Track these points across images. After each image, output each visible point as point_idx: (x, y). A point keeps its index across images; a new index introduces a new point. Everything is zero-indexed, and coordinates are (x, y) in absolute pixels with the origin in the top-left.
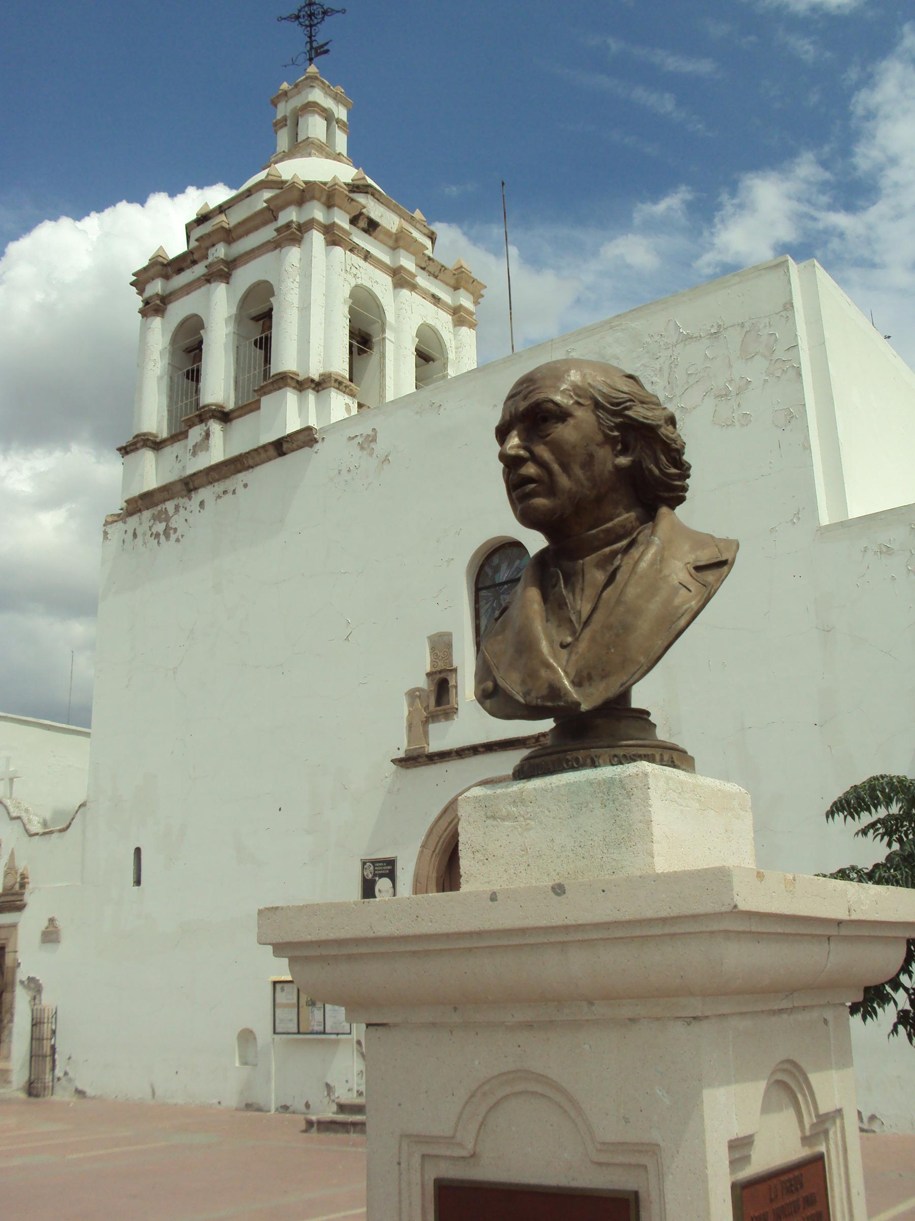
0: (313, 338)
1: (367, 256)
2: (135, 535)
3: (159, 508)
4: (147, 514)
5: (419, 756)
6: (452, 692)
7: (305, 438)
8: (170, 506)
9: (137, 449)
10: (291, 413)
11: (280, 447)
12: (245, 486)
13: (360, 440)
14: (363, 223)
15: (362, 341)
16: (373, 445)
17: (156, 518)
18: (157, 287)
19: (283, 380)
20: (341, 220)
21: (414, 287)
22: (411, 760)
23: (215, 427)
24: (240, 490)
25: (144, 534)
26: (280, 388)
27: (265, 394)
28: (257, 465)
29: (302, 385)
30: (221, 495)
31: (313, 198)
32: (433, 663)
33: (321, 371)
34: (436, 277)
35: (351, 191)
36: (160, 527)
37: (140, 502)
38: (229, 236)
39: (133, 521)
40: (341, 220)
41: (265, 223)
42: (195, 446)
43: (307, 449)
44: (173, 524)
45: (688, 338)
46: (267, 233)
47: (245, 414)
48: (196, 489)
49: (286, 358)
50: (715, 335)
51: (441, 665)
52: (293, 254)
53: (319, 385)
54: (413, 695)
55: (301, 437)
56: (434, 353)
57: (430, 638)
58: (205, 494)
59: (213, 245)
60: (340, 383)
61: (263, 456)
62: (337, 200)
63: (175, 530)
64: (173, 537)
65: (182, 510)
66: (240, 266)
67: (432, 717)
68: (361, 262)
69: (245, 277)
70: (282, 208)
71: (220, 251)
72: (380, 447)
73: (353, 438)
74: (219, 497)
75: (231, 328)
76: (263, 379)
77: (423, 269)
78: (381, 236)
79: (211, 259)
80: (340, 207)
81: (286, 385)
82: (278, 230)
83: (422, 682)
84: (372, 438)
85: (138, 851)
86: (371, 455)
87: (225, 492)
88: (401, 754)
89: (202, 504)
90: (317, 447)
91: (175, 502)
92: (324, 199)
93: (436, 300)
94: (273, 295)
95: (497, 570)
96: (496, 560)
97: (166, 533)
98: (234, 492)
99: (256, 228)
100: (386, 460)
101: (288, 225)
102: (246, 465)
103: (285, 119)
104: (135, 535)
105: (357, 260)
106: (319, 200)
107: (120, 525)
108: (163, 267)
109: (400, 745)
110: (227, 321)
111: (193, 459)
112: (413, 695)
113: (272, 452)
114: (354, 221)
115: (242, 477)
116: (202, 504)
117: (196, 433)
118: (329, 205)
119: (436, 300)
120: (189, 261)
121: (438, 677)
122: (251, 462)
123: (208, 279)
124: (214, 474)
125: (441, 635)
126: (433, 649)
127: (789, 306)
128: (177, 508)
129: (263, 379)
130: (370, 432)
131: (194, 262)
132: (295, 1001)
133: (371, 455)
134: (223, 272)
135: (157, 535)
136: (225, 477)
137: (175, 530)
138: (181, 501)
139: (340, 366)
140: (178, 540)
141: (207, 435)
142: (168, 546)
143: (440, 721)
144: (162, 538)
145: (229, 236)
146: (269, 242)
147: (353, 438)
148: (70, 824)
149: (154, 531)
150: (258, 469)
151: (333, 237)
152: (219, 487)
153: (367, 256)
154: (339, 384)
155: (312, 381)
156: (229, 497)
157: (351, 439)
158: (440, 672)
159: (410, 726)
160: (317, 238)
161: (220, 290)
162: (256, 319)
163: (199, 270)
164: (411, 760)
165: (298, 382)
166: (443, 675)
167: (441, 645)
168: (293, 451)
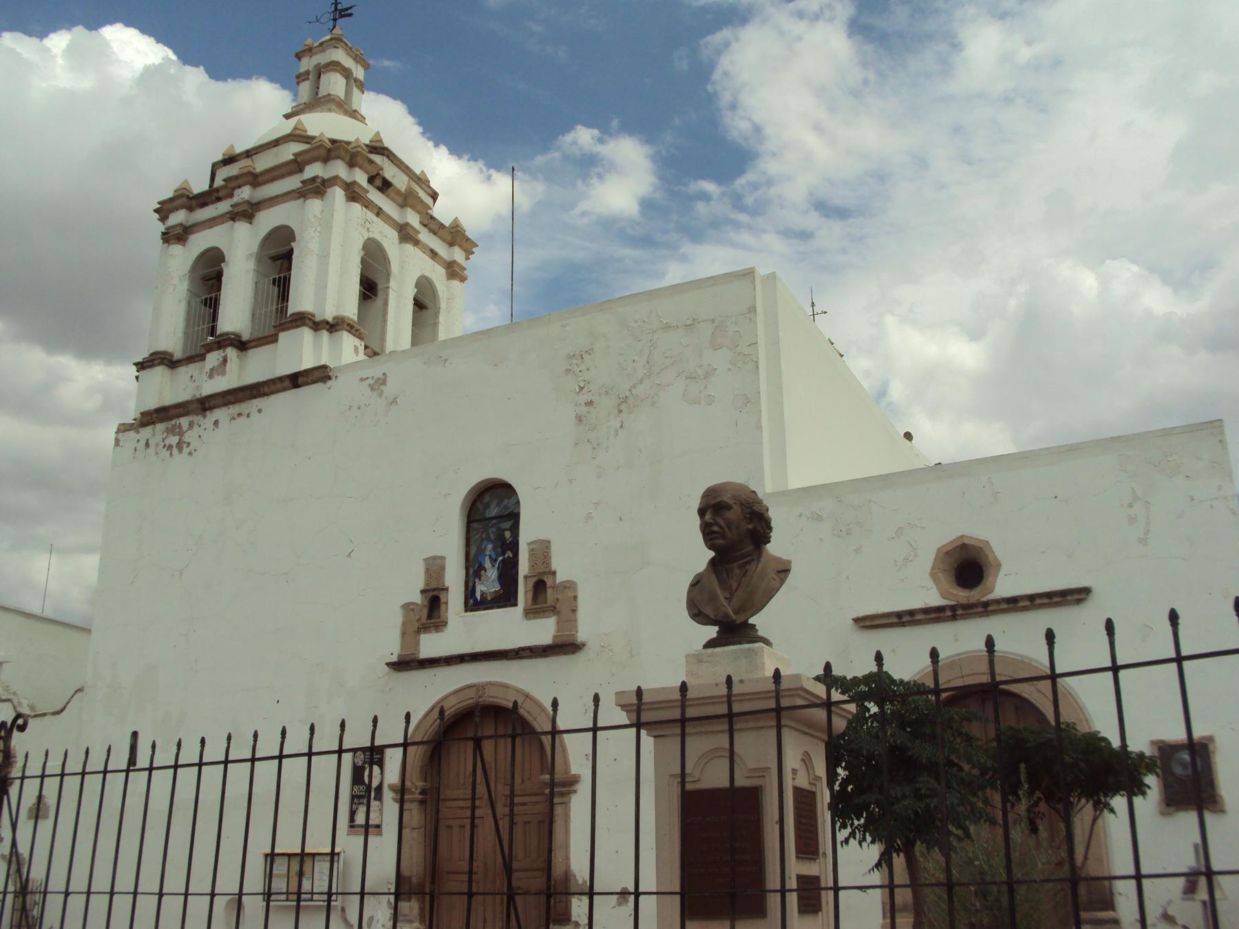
0: (325, 284)
1: (379, 212)
2: (147, 445)
3: (173, 422)
4: (160, 427)
5: (412, 661)
6: (443, 607)
7: (320, 375)
8: (184, 421)
10: (301, 349)
11: (296, 380)
12: (260, 411)
13: (371, 381)
14: (378, 182)
15: (370, 289)
16: (382, 387)
17: (171, 431)
18: (178, 217)
19: (301, 319)
20: (361, 178)
21: (416, 243)
22: (405, 664)
23: (231, 352)
24: (254, 414)
26: (298, 327)
27: (283, 330)
28: (273, 393)
29: (318, 326)
31: (338, 157)
32: (427, 582)
33: (335, 314)
34: (435, 234)
35: (371, 152)
36: (174, 440)
38: (256, 180)
39: (146, 432)
40: (361, 178)
41: (290, 173)
42: (212, 370)
43: (320, 384)
44: (186, 438)
45: (668, 327)
46: (293, 183)
48: (211, 408)
49: (302, 299)
50: (689, 327)
51: (433, 585)
52: (315, 205)
53: (333, 326)
56: (427, 302)
58: (220, 414)
60: (352, 327)
61: (279, 386)
62: (359, 160)
63: (189, 444)
64: (186, 450)
65: (196, 428)
67: (424, 629)
68: (374, 217)
69: (268, 220)
70: (310, 162)
71: (245, 193)
72: (389, 390)
74: (233, 418)
75: (251, 265)
76: (280, 317)
77: (425, 226)
78: (393, 195)
79: (235, 200)
80: (361, 168)
81: (304, 324)
82: (303, 182)
83: (417, 598)
84: (383, 381)
85: (135, 734)
86: (380, 395)
87: (240, 415)
88: (394, 659)
89: (216, 423)
90: (330, 383)
91: (190, 418)
92: (348, 159)
93: (433, 254)
94: (293, 239)
95: (487, 506)
96: (487, 498)
97: (180, 446)
98: (248, 416)
99: (282, 177)
100: (394, 402)
101: (314, 179)
103: (307, 73)
104: (147, 445)
105: (371, 216)
106: (343, 159)
107: (132, 434)
108: (186, 200)
109: (393, 650)
110: (249, 257)
111: (210, 382)
112: (408, 607)
113: (287, 383)
114: (371, 180)
115: (257, 403)
116: (216, 423)
117: (213, 358)
118: (351, 164)
119: (433, 254)
121: (431, 594)
122: (266, 390)
123: (233, 216)
124: (231, 398)
125: (435, 558)
126: (427, 570)
127: (753, 309)
128: (191, 425)
129: (280, 317)
130: (381, 376)
131: (219, 199)
132: (285, 871)
133: (380, 395)
134: (247, 213)
135: (170, 447)
136: (241, 401)
137: (189, 444)
138: (197, 419)
139: (350, 310)
140: (190, 454)
141: (225, 361)
142: (180, 459)
144: (175, 451)
145: (256, 180)
146: (293, 191)
148: (64, 708)
149: (167, 442)
150: (272, 397)
151: (353, 194)
152: (234, 409)
153: (379, 212)
154: (351, 328)
155: (327, 323)
156: (242, 420)
157: (362, 380)
158: (434, 590)
159: (404, 634)
160: (338, 193)
161: (242, 227)
162: (274, 258)
163: (224, 207)
164: (405, 664)
165: (314, 322)
167: (435, 567)
168: (307, 384)
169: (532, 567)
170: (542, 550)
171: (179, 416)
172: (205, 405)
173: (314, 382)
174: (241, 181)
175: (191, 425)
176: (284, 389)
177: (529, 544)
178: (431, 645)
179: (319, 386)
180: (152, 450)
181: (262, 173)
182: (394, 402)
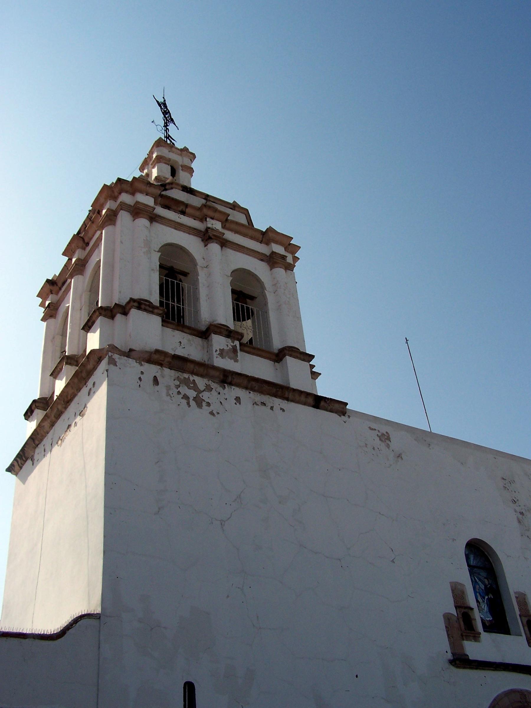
2: (156, 381)
3: (186, 376)
8: (201, 382)
9: (152, 312)
11: (319, 402)
17: (186, 382)
25: (168, 388)
28: (292, 401)
30: (259, 403)
36: (192, 394)
37: (168, 359)
39: (152, 370)
47: (253, 354)
48: (231, 384)
54: (447, 617)
55: (337, 406)
57: (450, 583)
59: (212, 218)
65: (214, 392)
66: (229, 248)
71: (217, 225)
73: (372, 429)
74: (255, 403)
81: (284, 356)
87: (263, 404)
100: (399, 456)
102: (286, 396)
104: (156, 381)
111: (220, 358)
112: (447, 617)
113: (310, 400)
115: (277, 402)
120: (180, 209)
121: (463, 610)
122: (291, 396)
124: (266, 387)
131: (183, 213)
135: (185, 397)
136: (261, 392)
137: (209, 404)
138: (214, 385)
140: (212, 413)
143: (471, 640)
144: (192, 403)
147: (372, 429)
152: (259, 398)
156: (267, 409)
157: (370, 428)
166: (466, 610)
169: (520, 610)
170: (522, 600)
171: (193, 373)
172: (227, 378)
173: (331, 411)
174: (217, 215)
175: (209, 389)
176: (305, 404)
177: (515, 593)
178: (478, 649)
179: (334, 416)
180: (161, 388)
181: (233, 222)
182: (399, 456)
